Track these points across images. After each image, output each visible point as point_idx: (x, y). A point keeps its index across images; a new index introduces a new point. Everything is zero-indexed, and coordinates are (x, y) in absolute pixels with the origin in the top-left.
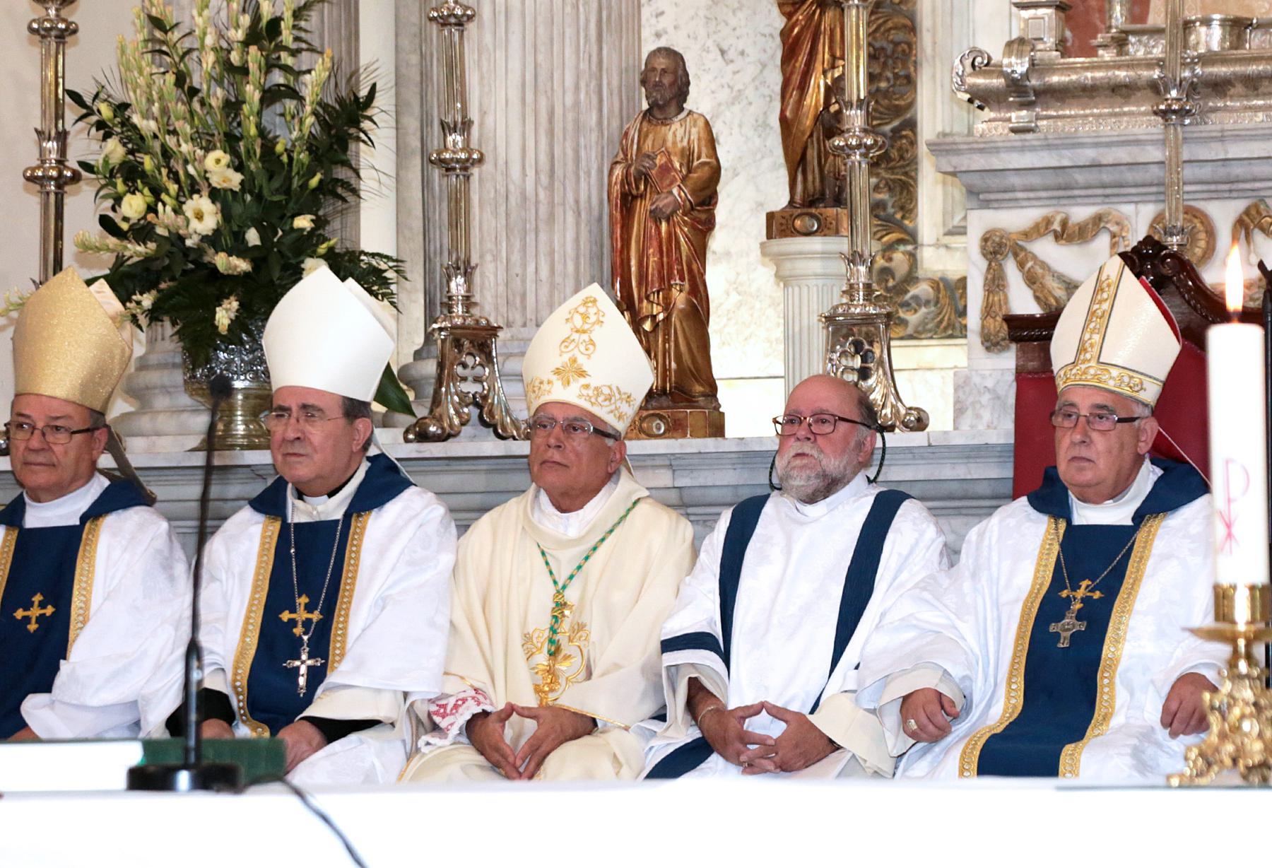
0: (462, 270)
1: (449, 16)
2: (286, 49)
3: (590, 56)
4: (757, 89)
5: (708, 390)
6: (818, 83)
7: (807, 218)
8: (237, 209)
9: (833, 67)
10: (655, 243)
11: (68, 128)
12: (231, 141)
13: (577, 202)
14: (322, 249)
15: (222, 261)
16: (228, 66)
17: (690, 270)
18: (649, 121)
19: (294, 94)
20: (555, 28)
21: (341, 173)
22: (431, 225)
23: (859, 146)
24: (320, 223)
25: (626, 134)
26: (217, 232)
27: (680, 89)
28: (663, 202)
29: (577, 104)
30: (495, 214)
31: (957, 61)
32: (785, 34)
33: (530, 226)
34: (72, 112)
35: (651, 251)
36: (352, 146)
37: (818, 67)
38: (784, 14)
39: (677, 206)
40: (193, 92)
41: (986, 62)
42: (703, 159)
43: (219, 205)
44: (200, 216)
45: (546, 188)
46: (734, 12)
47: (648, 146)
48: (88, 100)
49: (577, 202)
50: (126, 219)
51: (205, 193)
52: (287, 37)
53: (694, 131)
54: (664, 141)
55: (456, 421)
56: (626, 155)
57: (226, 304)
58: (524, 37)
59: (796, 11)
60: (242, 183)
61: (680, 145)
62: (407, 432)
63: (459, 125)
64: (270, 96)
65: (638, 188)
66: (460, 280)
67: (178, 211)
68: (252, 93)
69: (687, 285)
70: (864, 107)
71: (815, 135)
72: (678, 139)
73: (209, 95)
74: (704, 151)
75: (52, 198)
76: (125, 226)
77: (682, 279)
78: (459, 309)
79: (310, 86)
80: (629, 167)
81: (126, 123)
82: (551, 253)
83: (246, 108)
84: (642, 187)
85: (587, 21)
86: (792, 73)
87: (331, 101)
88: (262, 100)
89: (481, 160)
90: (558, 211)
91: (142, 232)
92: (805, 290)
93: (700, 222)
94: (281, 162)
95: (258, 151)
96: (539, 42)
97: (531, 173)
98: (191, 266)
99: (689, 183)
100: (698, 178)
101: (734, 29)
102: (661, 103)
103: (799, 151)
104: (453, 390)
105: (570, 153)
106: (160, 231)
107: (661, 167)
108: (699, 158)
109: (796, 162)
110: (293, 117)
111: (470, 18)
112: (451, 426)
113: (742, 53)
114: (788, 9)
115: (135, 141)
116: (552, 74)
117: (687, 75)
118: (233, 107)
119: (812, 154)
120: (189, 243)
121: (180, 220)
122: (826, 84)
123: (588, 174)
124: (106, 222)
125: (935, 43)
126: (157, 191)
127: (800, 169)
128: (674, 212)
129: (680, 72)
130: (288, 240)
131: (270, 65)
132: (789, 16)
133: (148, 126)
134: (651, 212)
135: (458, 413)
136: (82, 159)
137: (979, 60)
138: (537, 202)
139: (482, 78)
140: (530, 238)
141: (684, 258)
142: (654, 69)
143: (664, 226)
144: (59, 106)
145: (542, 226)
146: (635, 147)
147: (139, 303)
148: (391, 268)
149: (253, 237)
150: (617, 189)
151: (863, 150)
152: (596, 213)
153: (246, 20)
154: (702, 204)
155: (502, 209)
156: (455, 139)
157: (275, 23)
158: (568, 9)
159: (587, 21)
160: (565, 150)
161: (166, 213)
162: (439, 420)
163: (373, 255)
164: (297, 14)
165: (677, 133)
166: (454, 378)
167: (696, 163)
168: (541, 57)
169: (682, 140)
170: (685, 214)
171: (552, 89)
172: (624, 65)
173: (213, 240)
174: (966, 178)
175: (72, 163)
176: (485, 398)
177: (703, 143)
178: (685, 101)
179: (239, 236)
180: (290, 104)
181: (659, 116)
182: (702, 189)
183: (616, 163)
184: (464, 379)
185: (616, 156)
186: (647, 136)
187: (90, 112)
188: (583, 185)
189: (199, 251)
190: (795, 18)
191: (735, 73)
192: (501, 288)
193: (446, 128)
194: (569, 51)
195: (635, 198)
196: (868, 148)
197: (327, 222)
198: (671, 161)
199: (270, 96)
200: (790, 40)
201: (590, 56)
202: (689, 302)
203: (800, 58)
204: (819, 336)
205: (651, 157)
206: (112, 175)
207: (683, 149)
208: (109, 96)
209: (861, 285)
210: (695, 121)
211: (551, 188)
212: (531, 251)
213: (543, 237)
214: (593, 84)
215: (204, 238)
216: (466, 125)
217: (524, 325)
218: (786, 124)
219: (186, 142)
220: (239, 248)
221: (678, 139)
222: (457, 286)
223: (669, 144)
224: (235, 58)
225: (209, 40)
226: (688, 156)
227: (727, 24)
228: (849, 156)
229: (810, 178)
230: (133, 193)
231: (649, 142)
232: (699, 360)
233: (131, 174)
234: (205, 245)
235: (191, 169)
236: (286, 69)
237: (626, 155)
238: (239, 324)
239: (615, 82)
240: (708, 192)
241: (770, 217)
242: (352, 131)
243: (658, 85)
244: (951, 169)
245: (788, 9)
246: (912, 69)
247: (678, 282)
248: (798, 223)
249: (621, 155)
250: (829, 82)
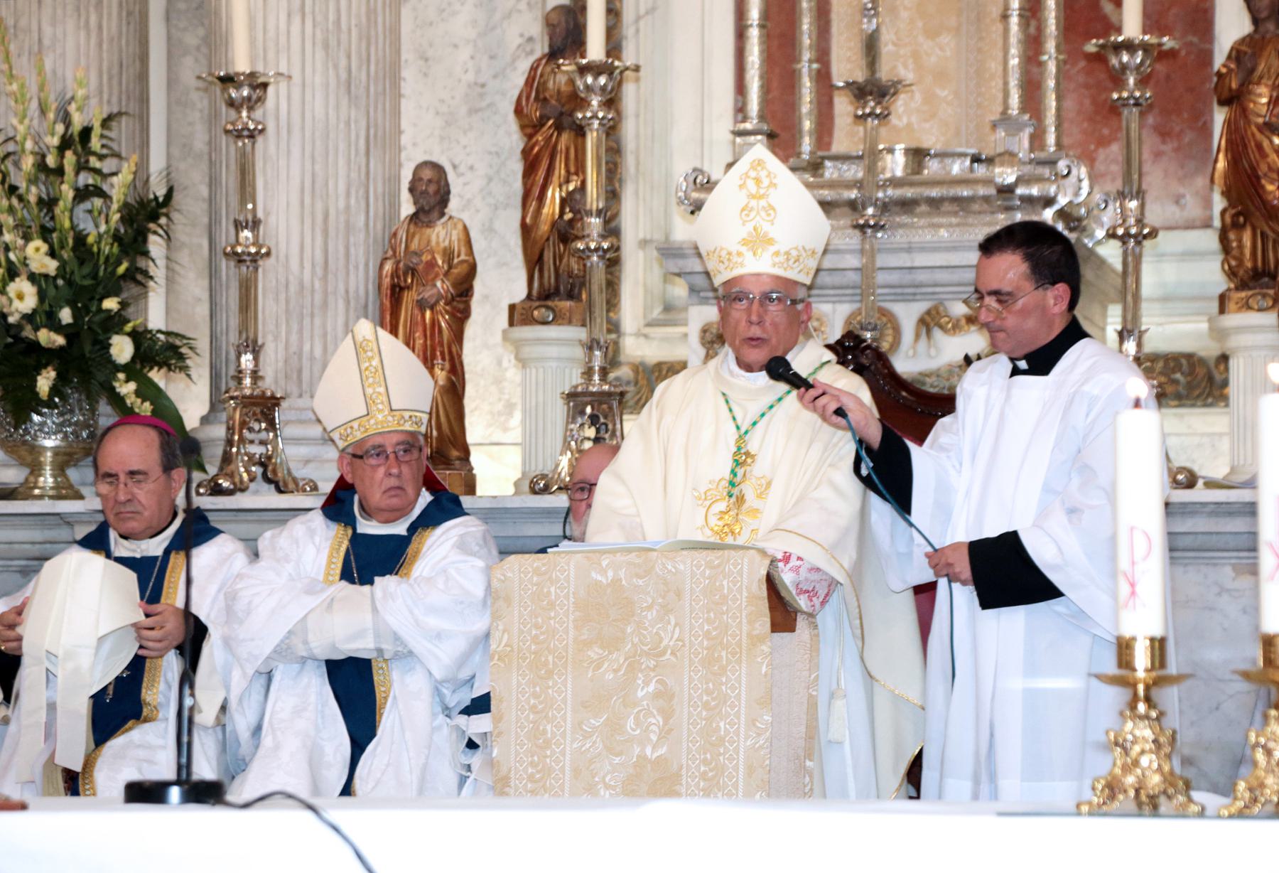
0: (251, 348)
1: (243, 129)
2: (94, 154)
3: (359, 168)
4: (484, 198)
5: (462, 455)
6: (554, 195)
7: (543, 310)
8: (52, 292)
9: (568, 181)
10: (420, 328)
12: (45, 233)
13: (347, 292)
14: (128, 328)
16: (41, 166)
17: (450, 352)
18: (416, 224)
22: (218, 308)
23: (596, 250)
24: (124, 305)
25: (395, 234)
26: (35, 311)
27: (442, 197)
28: (428, 293)
29: (348, 207)
30: (277, 300)
31: (682, 179)
32: (526, 153)
33: (306, 311)
35: (417, 335)
37: (555, 179)
38: (525, 135)
39: (440, 297)
41: (705, 181)
42: (463, 257)
44: (21, 297)
45: (320, 279)
46: (465, 133)
47: (414, 246)
49: (347, 292)
51: (24, 277)
52: (95, 143)
53: (455, 233)
54: (429, 242)
55: (245, 476)
56: (395, 252)
57: (44, 372)
58: (303, 149)
59: (536, 133)
60: (58, 269)
61: (442, 245)
63: (250, 224)
64: (82, 194)
65: (405, 281)
66: (249, 356)
68: (67, 192)
69: (447, 365)
70: (602, 215)
71: (551, 239)
74: (463, 250)
77: (443, 359)
78: (247, 381)
80: (398, 263)
82: (325, 335)
83: (61, 203)
84: (409, 281)
85: (357, 136)
86: (532, 185)
87: (130, 200)
88: (74, 198)
89: (268, 254)
90: (331, 299)
92: (541, 370)
93: (459, 311)
94: (92, 254)
95: (71, 241)
97: (308, 265)
98: (10, 340)
99: (450, 278)
100: (459, 274)
101: (465, 147)
102: (427, 208)
103: (537, 252)
104: (243, 451)
105: (341, 249)
107: (427, 262)
108: (459, 256)
109: (534, 262)
110: (100, 213)
111: (262, 131)
112: (241, 481)
113: (471, 168)
114: (529, 131)
117: (447, 185)
118: (48, 204)
119: (548, 256)
120: (11, 320)
122: (561, 197)
123: (357, 268)
125: (638, 164)
127: (537, 268)
128: (437, 302)
130: (97, 318)
131: (81, 167)
132: (530, 137)
134: (417, 301)
135: (248, 471)
137: (700, 178)
138: (313, 291)
139: (266, 183)
140: (307, 321)
141: (445, 341)
142: (421, 179)
143: (428, 314)
145: (316, 311)
146: (403, 246)
148: (185, 344)
149: (66, 315)
150: (387, 281)
151: (601, 253)
152: (362, 301)
153: (60, 128)
154: (461, 295)
155: (282, 297)
156: (246, 234)
157: (86, 133)
158: (342, 126)
159: (357, 136)
160: (338, 247)
162: (231, 476)
164: (106, 123)
165: (440, 235)
166: (242, 440)
167: (456, 261)
168: (317, 167)
169: (444, 241)
170: (446, 304)
171: (327, 195)
172: (387, 176)
173: (29, 318)
174: (688, 277)
176: (269, 458)
177: (462, 243)
178: (446, 206)
180: (98, 202)
181: (426, 220)
182: (461, 284)
183: (386, 259)
184: (252, 442)
185: (386, 252)
186: (413, 236)
188: (352, 277)
189: (19, 327)
190: (534, 140)
191: (465, 184)
192: (281, 364)
193: (238, 226)
194: (342, 162)
195: (402, 289)
196: (605, 251)
198: (434, 258)
199: (82, 194)
200: (531, 158)
201: (359, 168)
202: (449, 379)
203: (540, 173)
204: (559, 410)
205: (417, 254)
207: (445, 249)
209: (597, 368)
210: (455, 225)
211: (325, 278)
212: (306, 334)
213: (317, 321)
214: (362, 192)
216: (255, 224)
217: (300, 396)
218: (526, 230)
219: (9, 232)
220: (56, 327)
221: (441, 240)
223: (433, 243)
224: (51, 161)
225: (29, 145)
226: (449, 254)
227: (458, 142)
228: (589, 257)
229: (546, 275)
231: (416, 241)
232: (456, 429)
234: (24, 322)
235: (12, 256)
236: (97, 171)
237: (395, 252)
238: (55, 390)
239: (380, 190)
240: (465, 286)
241: (512, 308)
243: (424, 193)
244: (677, 271)
245: (529, 131)
246: (617, 185)
247: (440, 361)
248: (536, 313)
249: (390, 253)
250: (564, 194)
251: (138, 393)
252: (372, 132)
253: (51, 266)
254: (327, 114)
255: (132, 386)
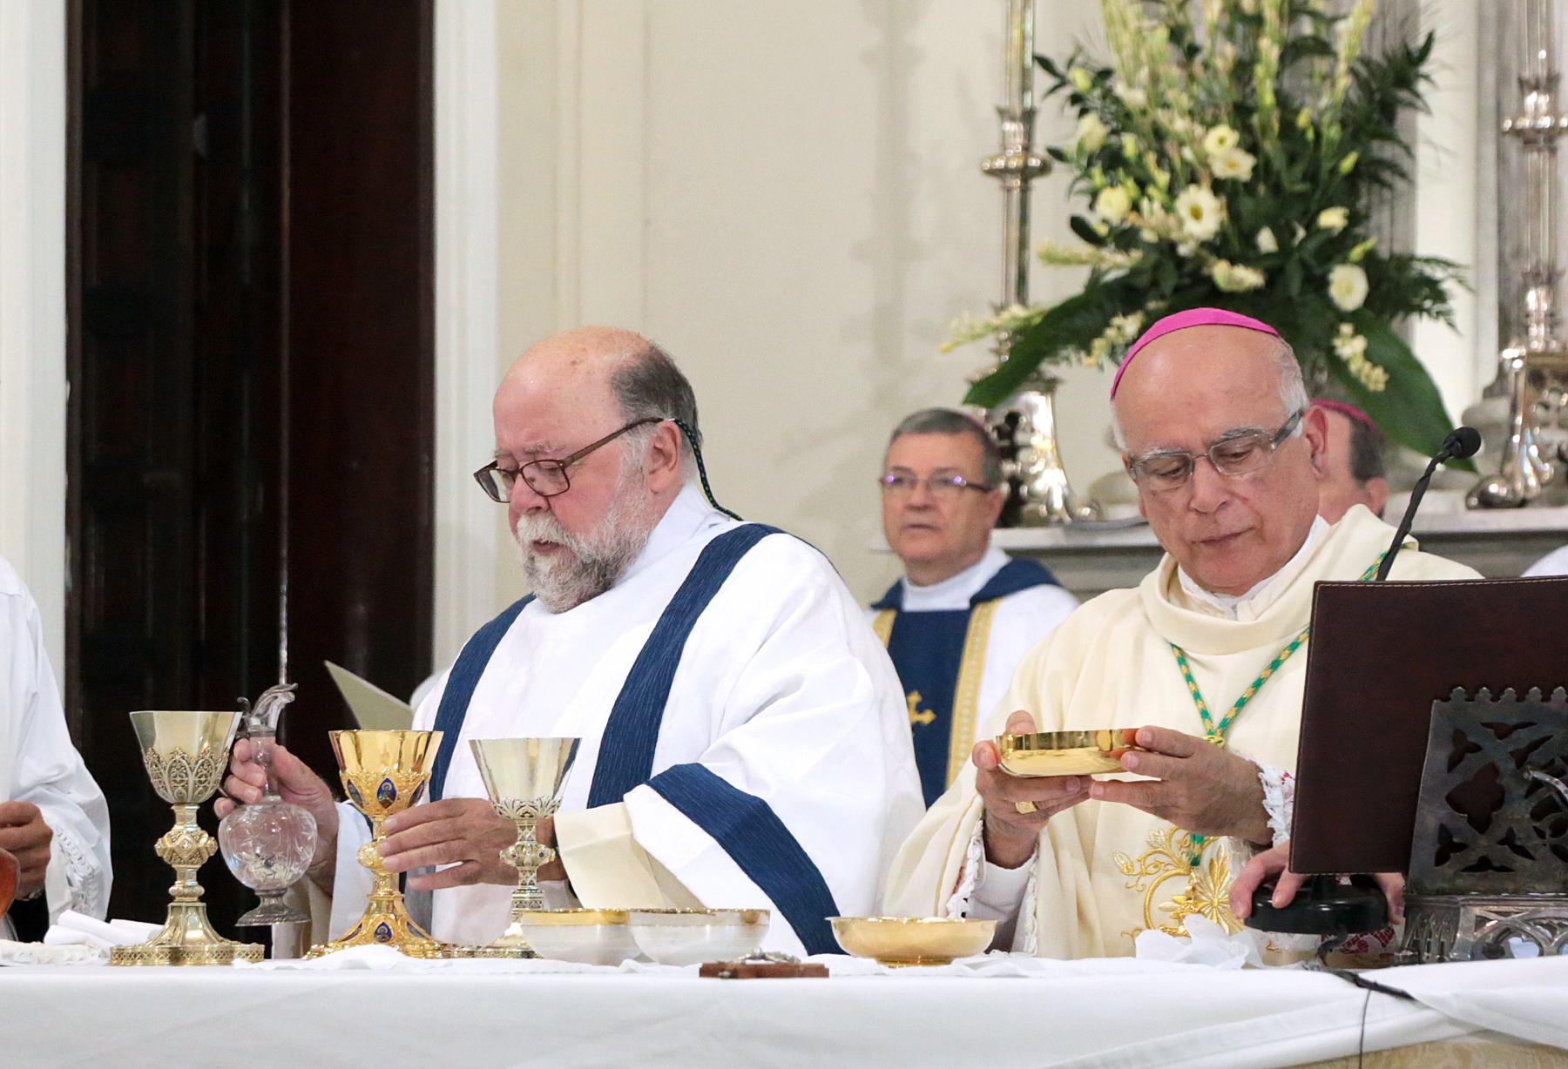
8: (1246, 204)
11: (1037, 104)
12: (1242, 114)
15: (1222, 272)
19: (1323, 48)
21: (1387, 151)
24: (1354, 219)
26: (1222, 234)
34: (1042, 80)
36: (1403, 115)
40: (1192, 51)
43: (1224, 199)
44: (1196, 214)
48: (1060, 66)
50: (1105, 221)
60: (1255, 169)
62: (1469, 495)
67: (1168, 209)
68: (1269, 49)
73: (1212, 54)
75: (1016, 194)
76: (1102, 230)
78: (1538, 331)
79: (1347, 37)
81: (1108, 94)
83: (1260, 70)
87: (1377, 56)
88: (1282, 58)
91: (1125, 238)
94: (1305, 142)
95: (1276, 126)
98: (1187, 281)
106: (1148, 236)
112: (1527, 488)
115: (1123, 119)
118: (1243, 70)
121: (1172, 221)
124: (1080, 227)
126: (1143, 183)
130: (1312, 245)
133: (1135, 97)
136: (1056, 144)
144: (1025, 74)
147: (1119, 328)
149: (1266, 240)
161: (1153, 208)
162: (1508, 479)
163: (1428, 261)
173: (1218, 247)
175: (1040, 150)
179: (1249, 238)
180: (1321, 65)
187: (1063, 82)
189: (1198, 262)
193: (1526, 86)
197: (1367, 217)
199: (1293, 51)
206: (1090, 164)
208: (1089, 58)
215: (1204, 245)
216: (1550, 84)
222: (1535, 300)
230: (1112, 185)
233: (1111, 159)
234: (1204, 253)
242: (1403, 94)
251: (1368, 355)
253: (1243, 166)
255: (1359, 344)
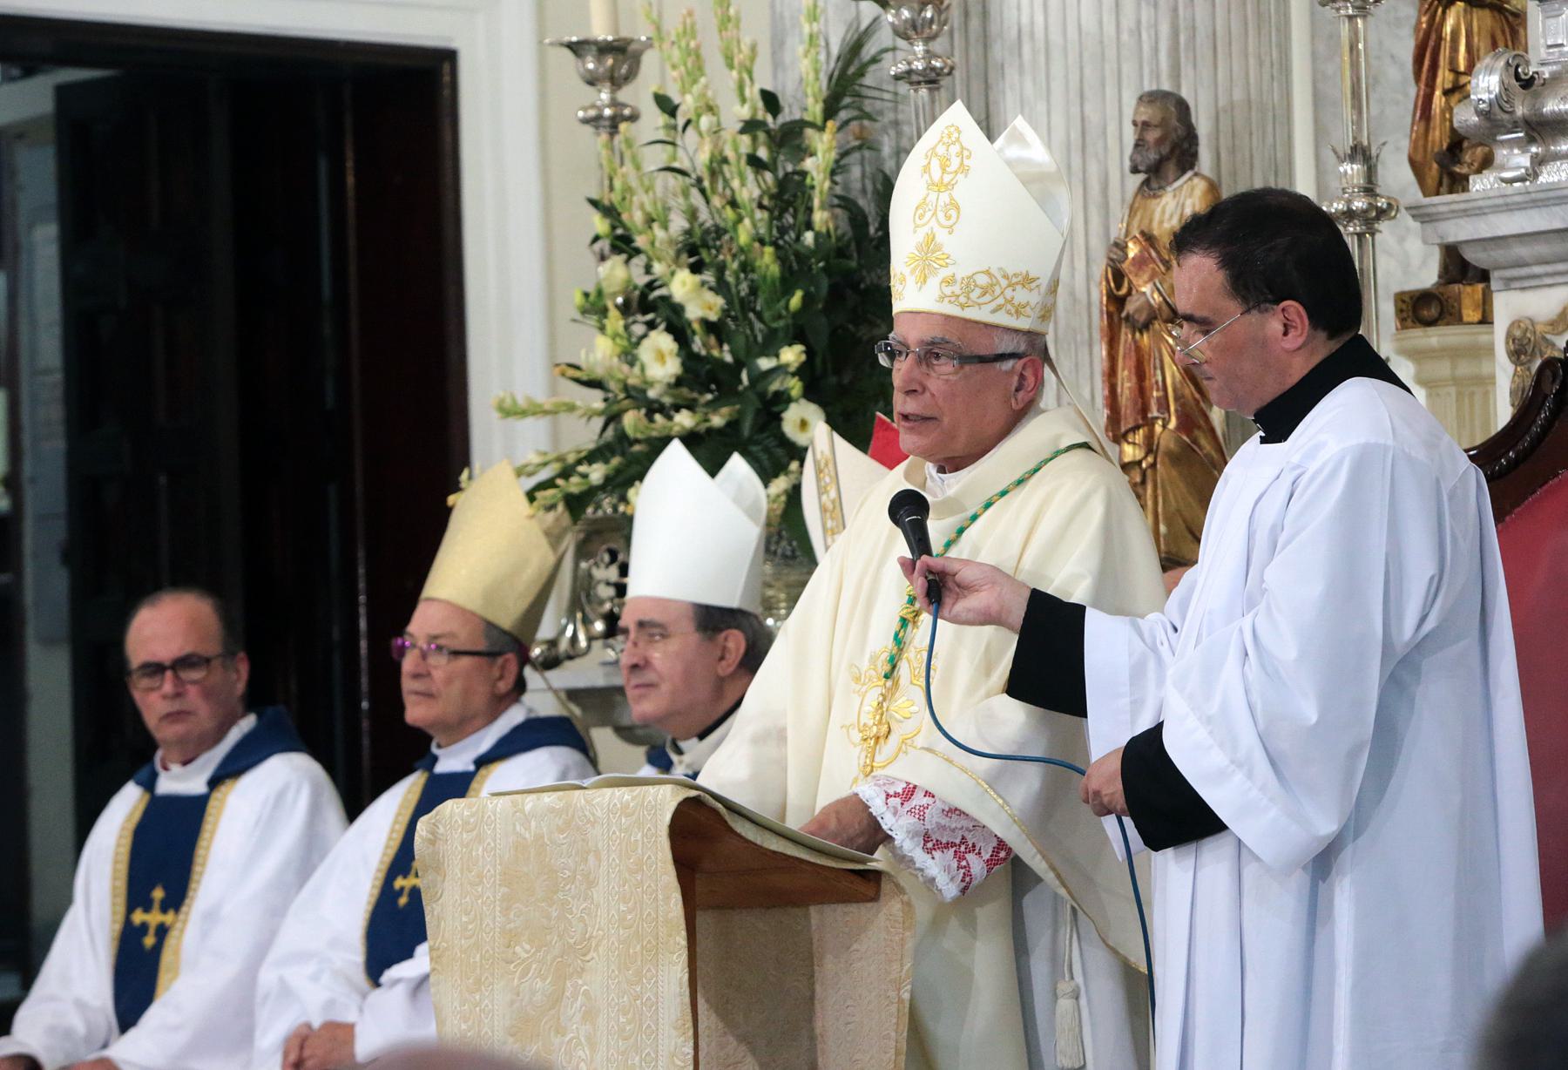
20: (1107, 66)
53: (1189, 202)
61: (1167, 226)
72: (1167, 216)
85: (1156, 50)
96: (1086, 88)
116: (1105, 128)
129: (1174, 122)
159: (1156, 50)
168: (1088, 108)
169: (1171, 216)
171: (1106, 148)
221: (1167, 216)
223: (1155, 225)
252: (1182, 38)
254: (1100, 23)
